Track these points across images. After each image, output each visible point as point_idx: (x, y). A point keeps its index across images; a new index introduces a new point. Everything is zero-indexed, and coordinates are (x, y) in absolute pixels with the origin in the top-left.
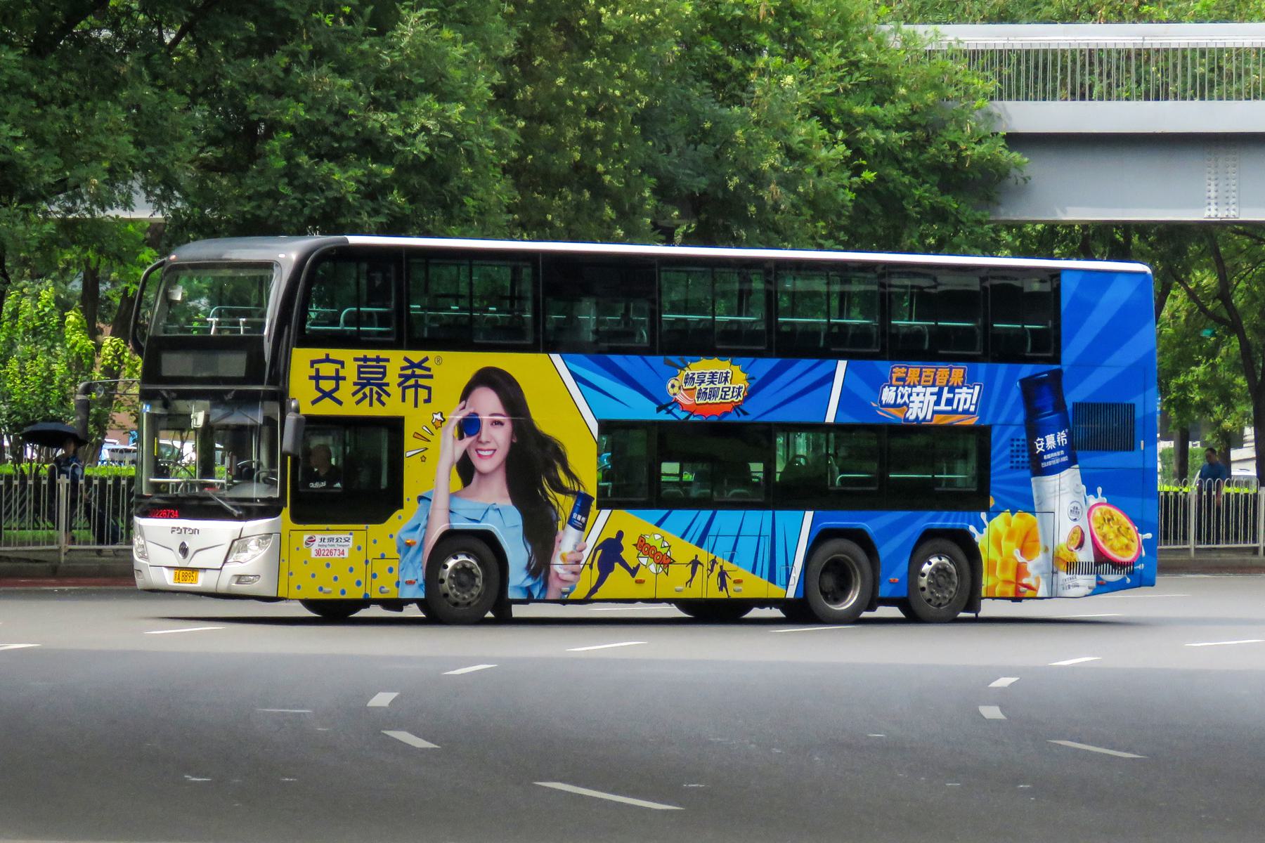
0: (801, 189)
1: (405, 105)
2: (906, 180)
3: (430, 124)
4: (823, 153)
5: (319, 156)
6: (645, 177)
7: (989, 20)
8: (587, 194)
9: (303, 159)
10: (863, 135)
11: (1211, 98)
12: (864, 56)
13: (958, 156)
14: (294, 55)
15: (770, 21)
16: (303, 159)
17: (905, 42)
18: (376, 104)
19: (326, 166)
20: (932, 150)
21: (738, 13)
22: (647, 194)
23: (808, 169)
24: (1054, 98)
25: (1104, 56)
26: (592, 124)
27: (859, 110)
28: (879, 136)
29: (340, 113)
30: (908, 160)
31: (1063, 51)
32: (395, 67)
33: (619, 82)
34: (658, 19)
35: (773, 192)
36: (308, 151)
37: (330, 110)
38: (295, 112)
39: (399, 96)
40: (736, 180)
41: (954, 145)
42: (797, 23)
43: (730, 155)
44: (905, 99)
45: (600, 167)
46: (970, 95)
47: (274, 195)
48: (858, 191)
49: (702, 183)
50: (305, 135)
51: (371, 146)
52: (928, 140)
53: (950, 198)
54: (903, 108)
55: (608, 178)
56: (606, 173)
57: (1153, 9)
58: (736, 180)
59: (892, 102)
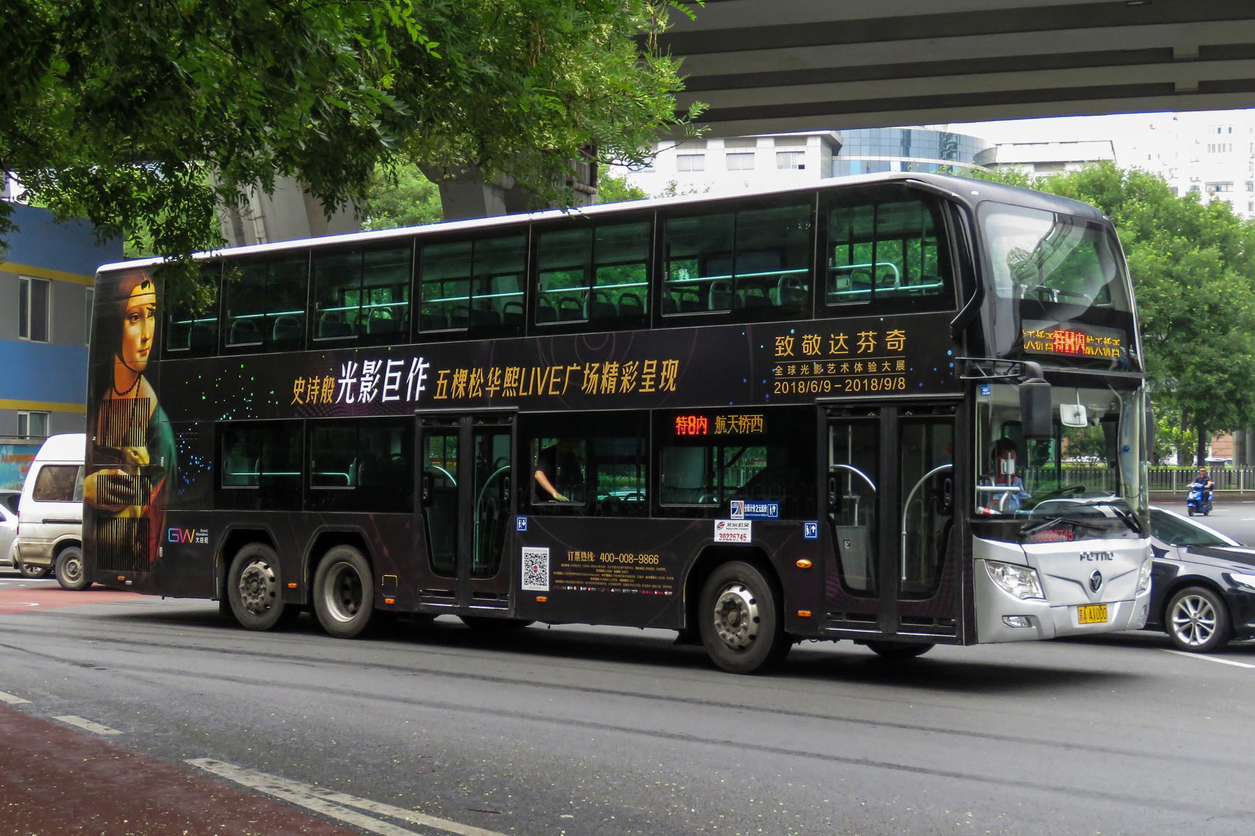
1: (1233, 355)
3: (1239, 361)
5: (1204, 372)
9: (1199, 374)
14: (1196, 342)
16: (1199, 374)
18: (1223, 356)
19: (1206, 375)
29: (1211, 359)
32: (1229, 345)
36: (1201, 371)
37: (1207, 358)
38: (1197, 359)
39: (1231, 353)
47: (1189, 385)
50: (1199, 366)
51: (1221, 369)
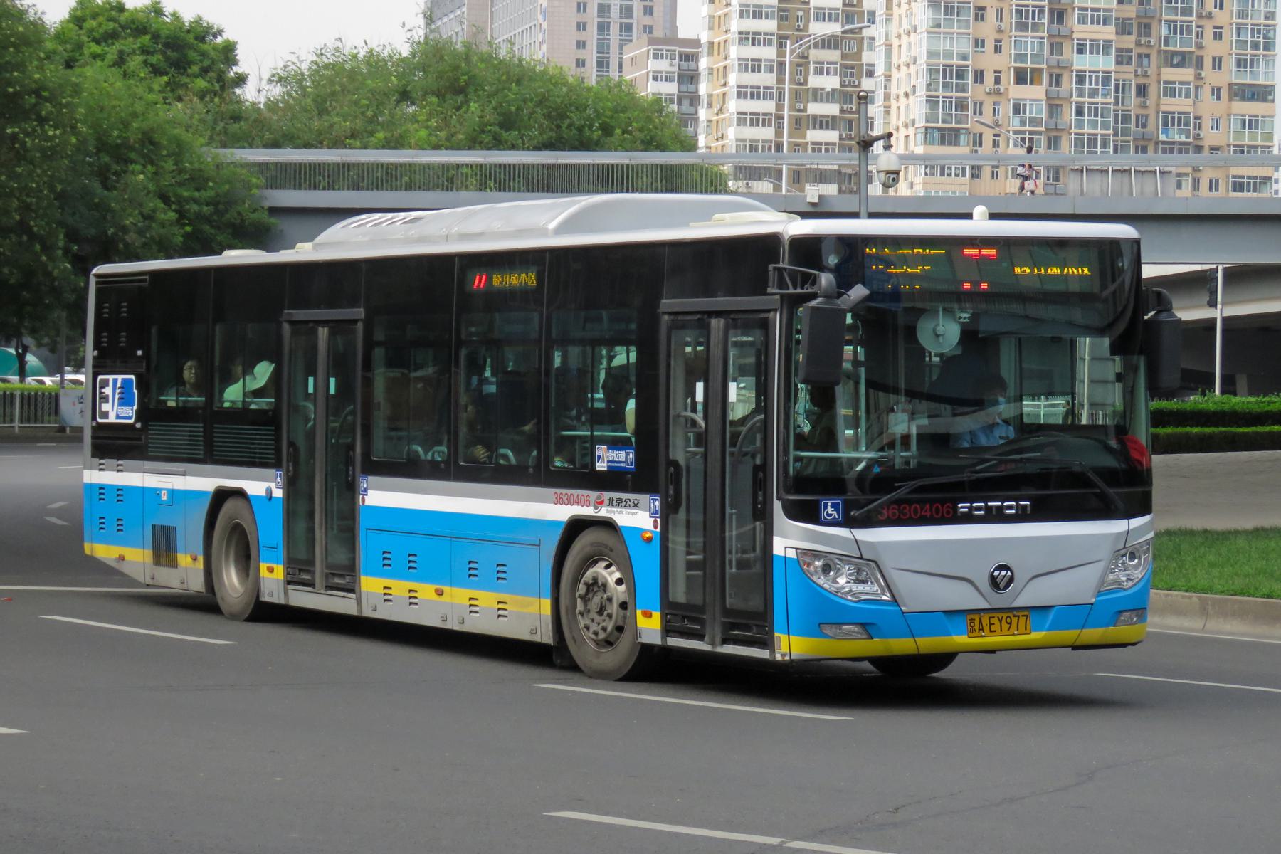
0: (148, 235)
2: (213, 231)
4: (162, 216)
6: (60, 229)
7: (266, 146)
8: (25, 238)
10: (187, 207)
11: (382, 189)
12: (187, 165)
13: (242, 220)
15: (137, 146)
17: (213, 159)
20: (228, 216)
21: (119, 141)
22: (61, 236)
23: (154, 225)
24: (300, 189)
25: (326, 167)
26: (28, 200)
27: (186, 194)
28: (195, 207)
30: (215, 221)
31: (315, 164)
33: (37, 179)
34: (57, 145)
35: (131, 237)
40: (112, 230)
41: (239, 213)
42: (152, 147)
43: (109, 218)
44: (212, 188)
45: (32, 223)
46: (249, 187)
48: (182, 236)
49: (93, 231)
52: (226, 211)
53: (236, 241)
54: (210, 193)
55: (35, 229)
56: (36, 226)
57: (352, 141)
58: (112, 230)
59: (206, 190)
